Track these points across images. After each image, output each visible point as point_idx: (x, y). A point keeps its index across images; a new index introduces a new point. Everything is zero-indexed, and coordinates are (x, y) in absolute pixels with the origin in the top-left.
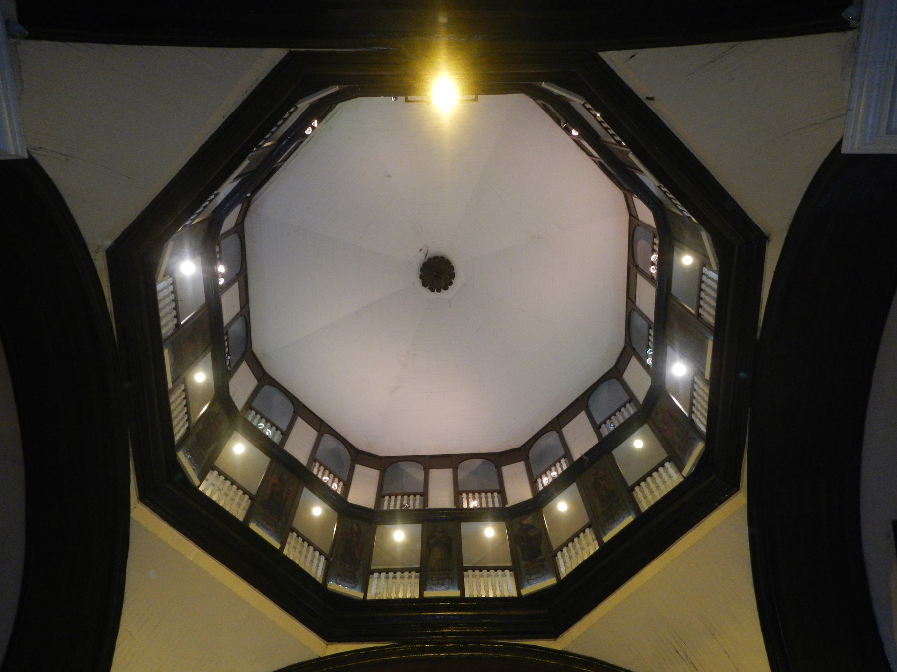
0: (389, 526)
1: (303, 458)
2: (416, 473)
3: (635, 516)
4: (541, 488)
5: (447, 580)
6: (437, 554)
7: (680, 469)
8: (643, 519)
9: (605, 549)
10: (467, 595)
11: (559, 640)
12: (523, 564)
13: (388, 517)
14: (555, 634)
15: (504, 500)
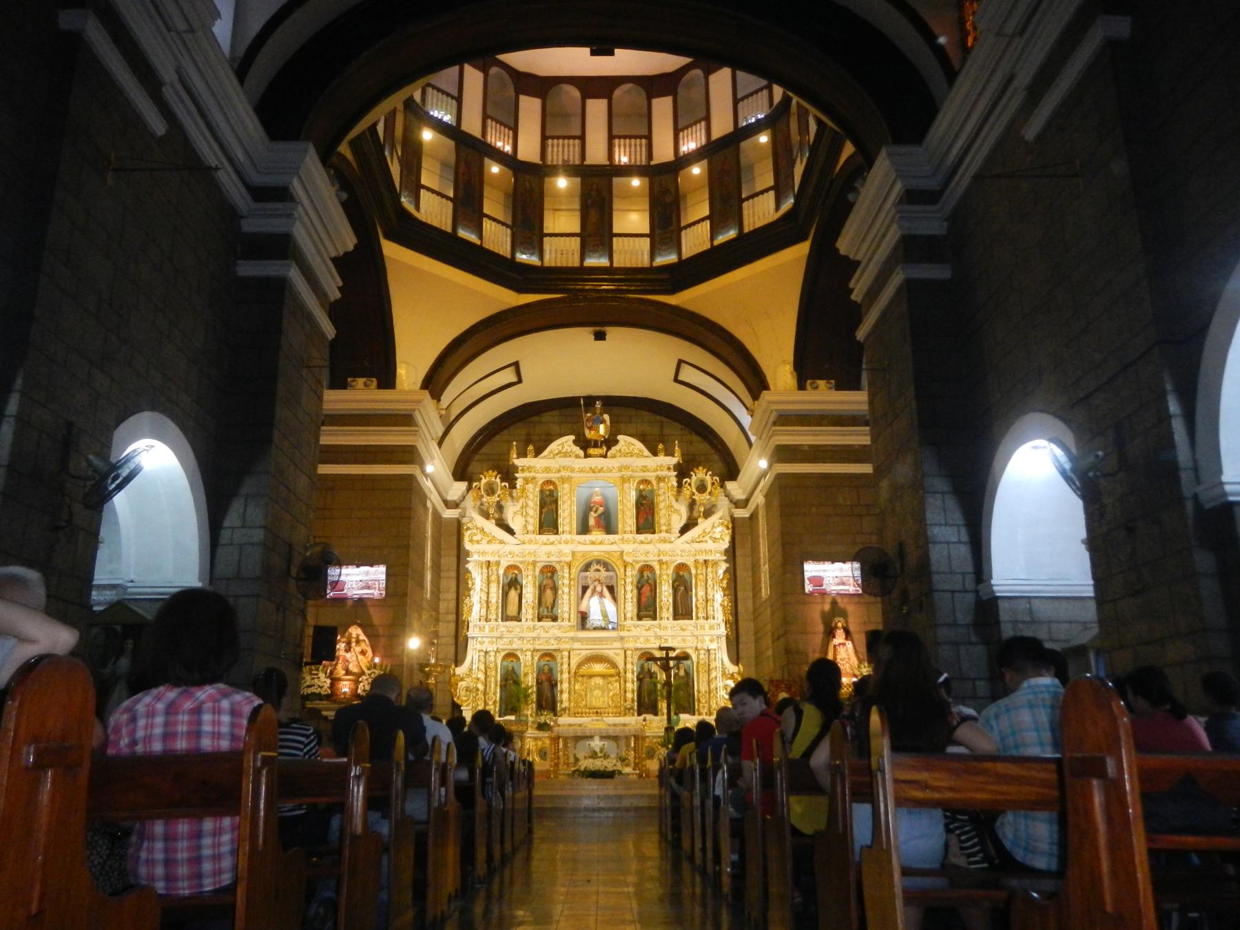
0: (553, 179)
1: (477, 133)
2: (575, 93)
3: (737, 232)
4: (682, 155)
5: (601, 247)
6: (593, 215)
7: (778, 208)
8: (741, 236)
9: (714, 250)
10: (615, 265)
11: (675, 296)
12: (658, 231)
13: (552, 171)
14: (673, 291)
15: (650, 155)
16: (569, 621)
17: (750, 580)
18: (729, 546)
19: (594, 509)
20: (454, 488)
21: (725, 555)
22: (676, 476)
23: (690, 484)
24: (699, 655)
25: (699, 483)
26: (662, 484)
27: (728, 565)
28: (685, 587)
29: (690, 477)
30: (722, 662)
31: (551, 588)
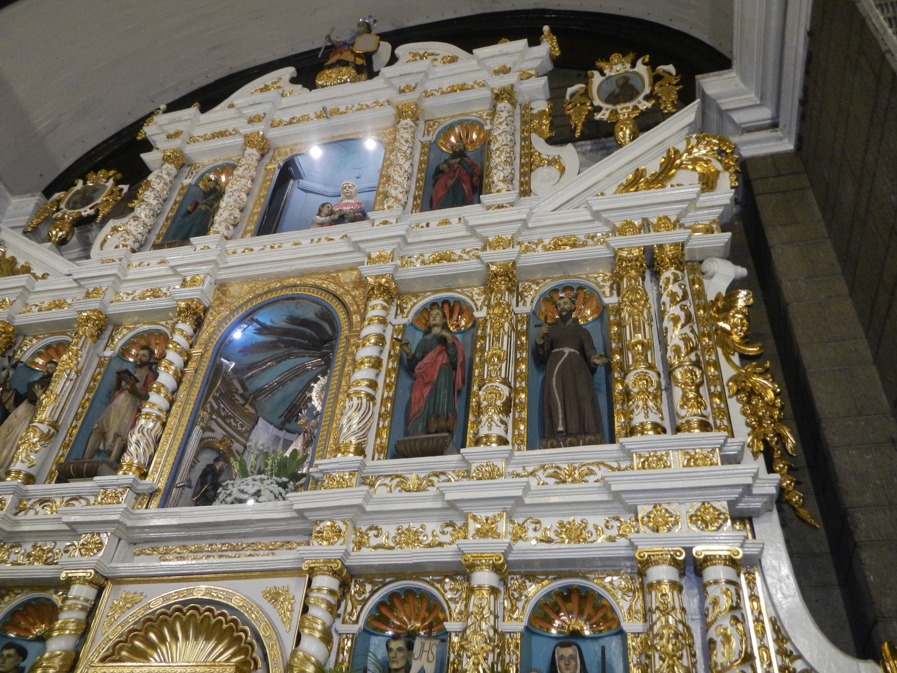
16: (144, 475)
17: (847, 307)
18: (736, 201)
19: (326, 210)
20: (9, 208)
21: (724, 229)
22: (548, 100)
23: (586, 93)
24: (647, 588)
25: (612, 87)
26: (503, 105)
27: (742, 271)
28: (582, 350)
29: (587, 80)
30: (781, 637)
31: (133, 392)
